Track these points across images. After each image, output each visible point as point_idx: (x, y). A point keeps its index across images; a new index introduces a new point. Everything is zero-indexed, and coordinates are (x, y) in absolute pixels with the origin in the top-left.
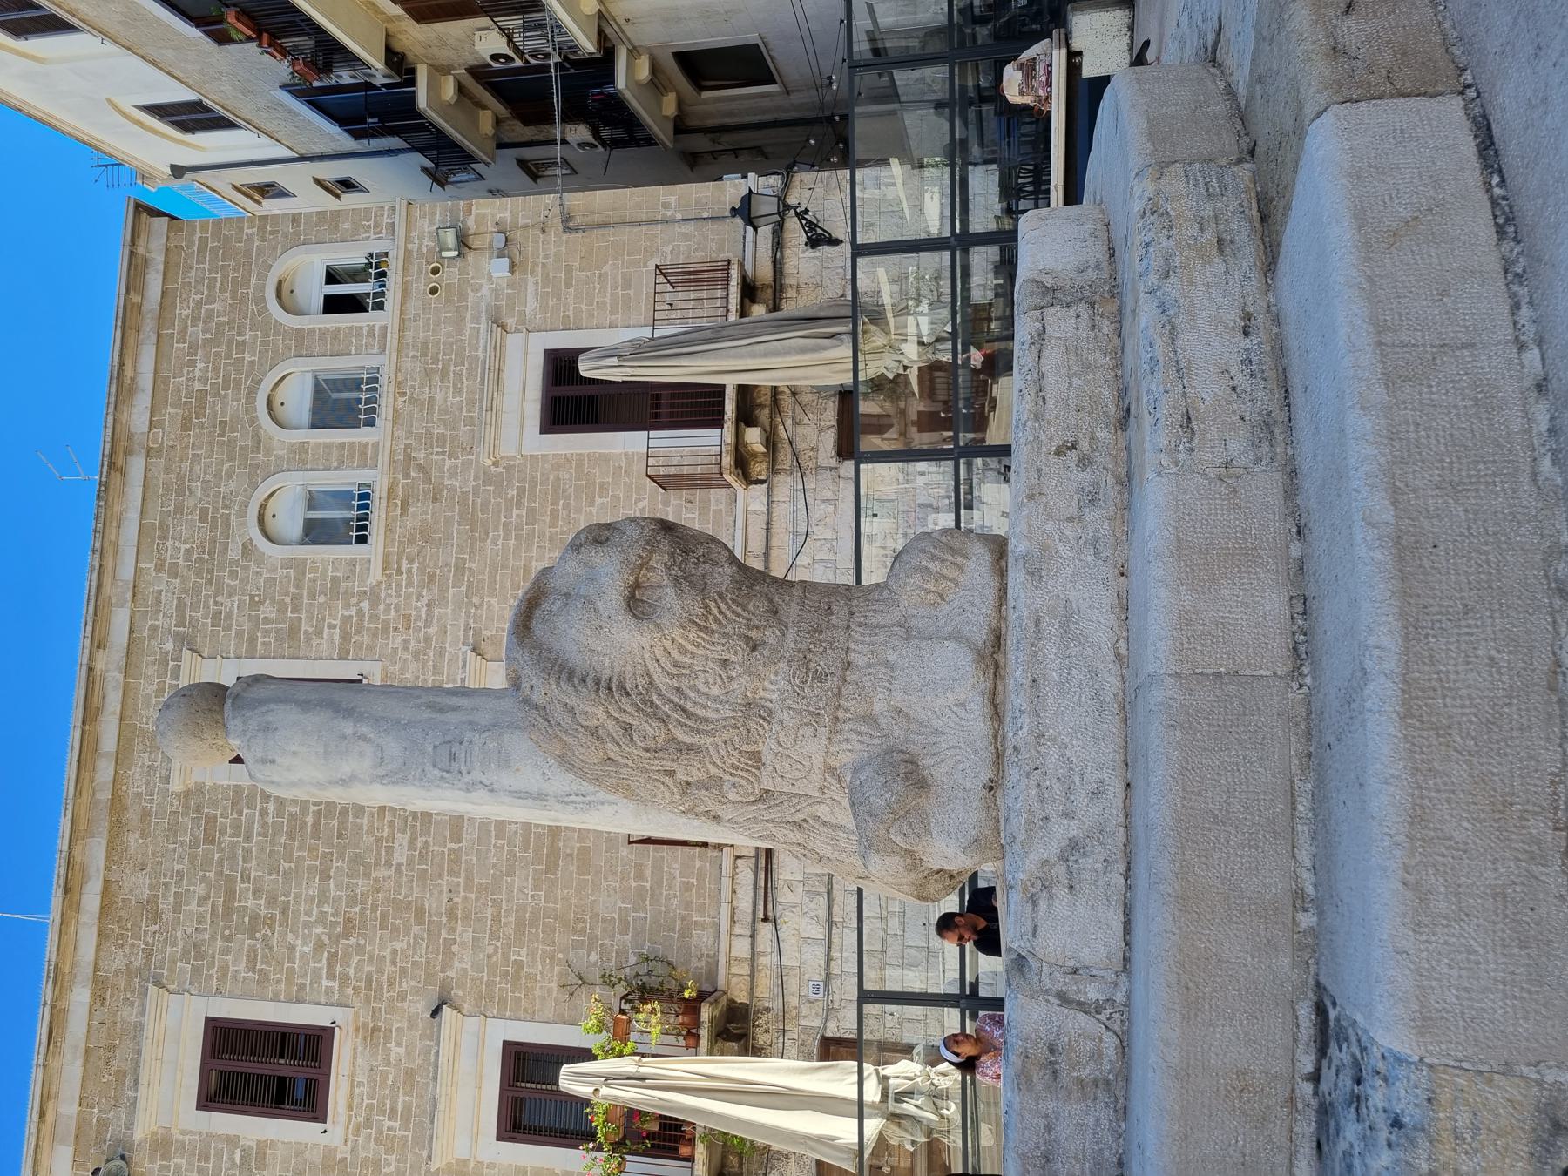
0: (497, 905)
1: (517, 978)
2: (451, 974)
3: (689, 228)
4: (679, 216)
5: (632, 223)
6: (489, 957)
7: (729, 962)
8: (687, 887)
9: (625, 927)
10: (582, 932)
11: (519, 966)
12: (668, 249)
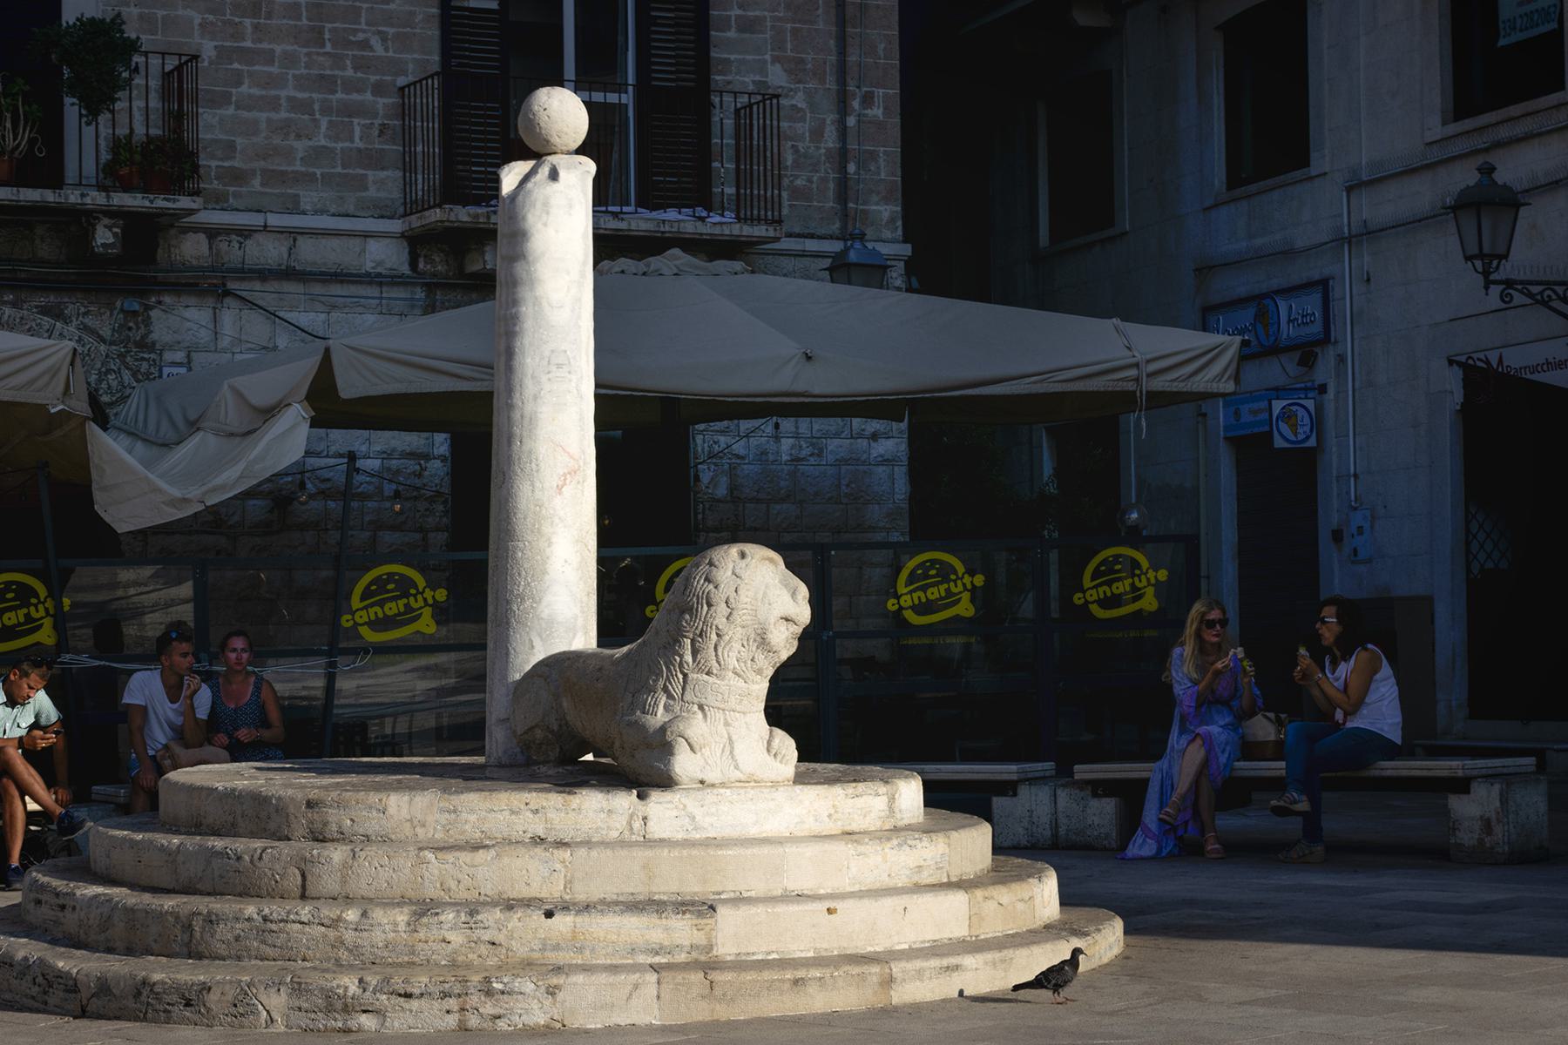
3: (830, 140)
4: (851, 121)
5: (842, 40)
12: (799, 100)
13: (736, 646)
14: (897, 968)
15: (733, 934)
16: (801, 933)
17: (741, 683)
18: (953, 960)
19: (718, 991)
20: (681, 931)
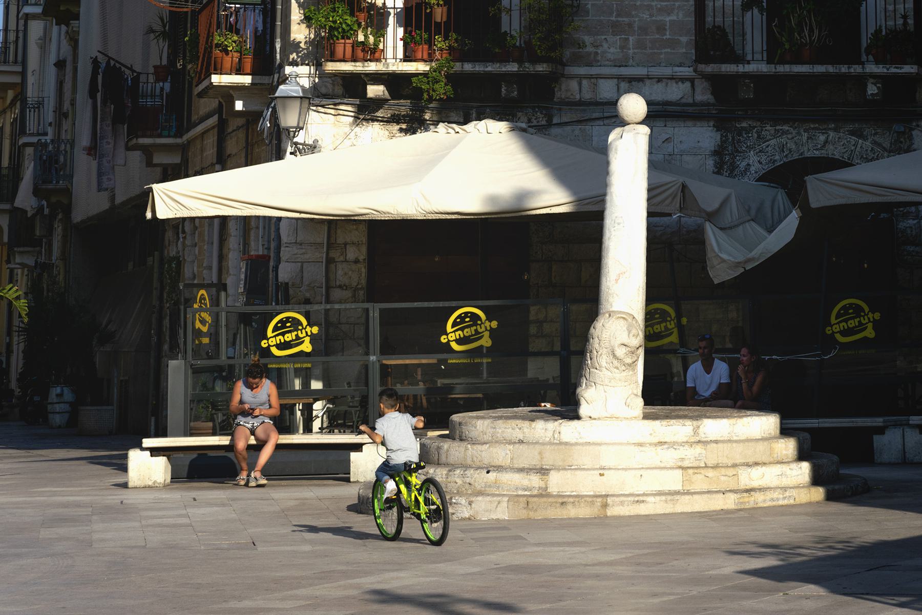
7: (590, 77)
8: (661, 28)
13: (604, 357)
14: (609, 500)
15: (557, 482)
16: (585, 483)
17: (609, 373)
18: (641, 498)
19: (530, 506)
20: (535, 481)
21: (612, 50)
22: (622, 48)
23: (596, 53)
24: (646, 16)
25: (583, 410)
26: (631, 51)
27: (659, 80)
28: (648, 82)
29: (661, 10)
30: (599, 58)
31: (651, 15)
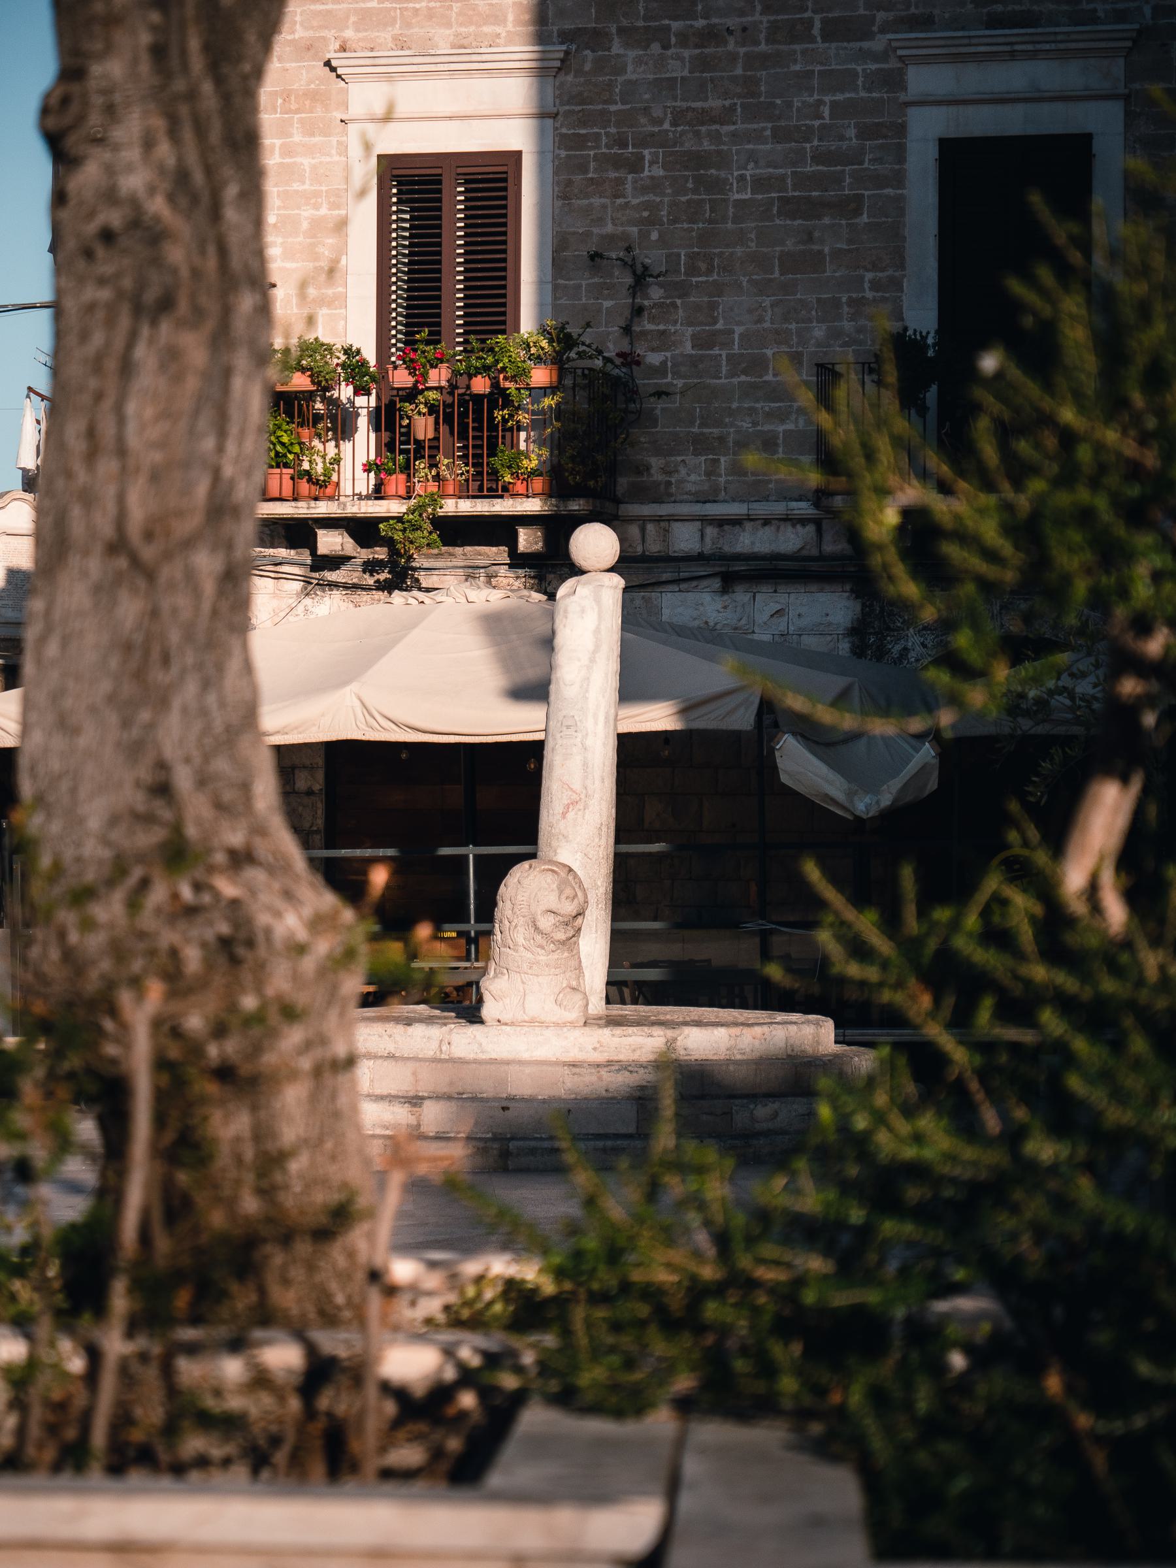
0: (725, 117)
1: (617, 162)
2: (616, 48)
6: (646, 110)
7: (658, 520)
9: (702, 342)
10: (692, 270)
11: (635, 165)
13: (521, 929)
17: (529, 955)
21: (693, 477)
22: (708, 474)
23: (669, 483)
24: (746, 425)
25: (487, 1011)
26: (722, 479)
27: (766, 522)
28: (748, 526)
29: (769, 415)
30: (673, 490)
31: (755, 424)
